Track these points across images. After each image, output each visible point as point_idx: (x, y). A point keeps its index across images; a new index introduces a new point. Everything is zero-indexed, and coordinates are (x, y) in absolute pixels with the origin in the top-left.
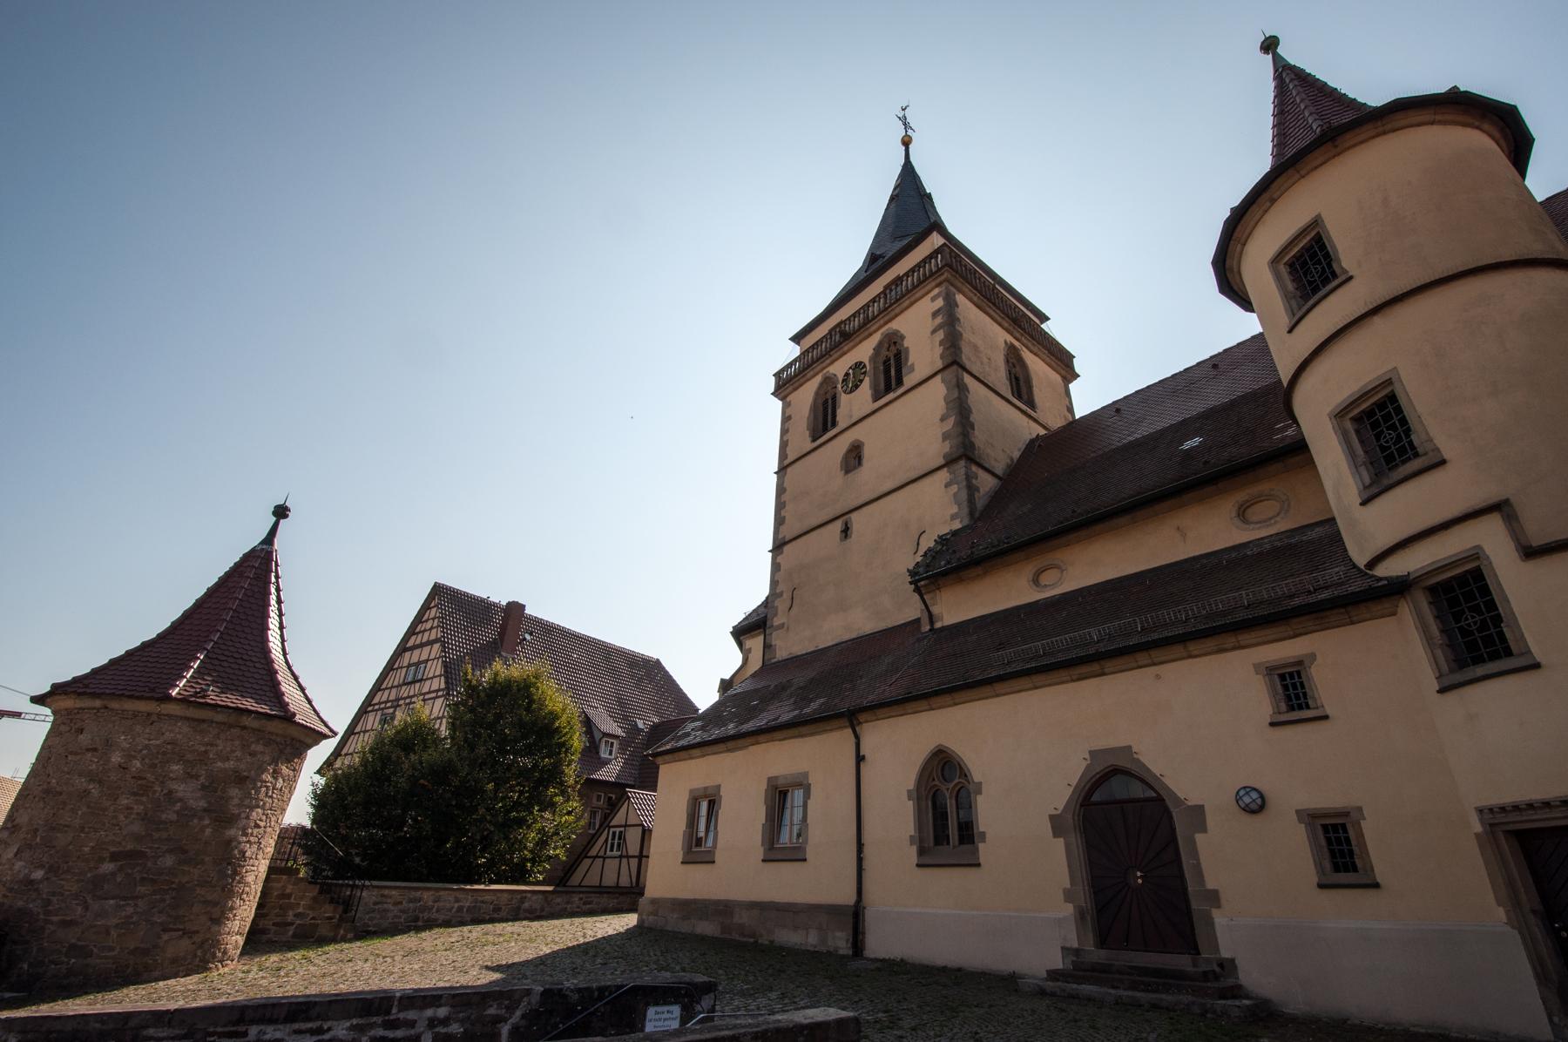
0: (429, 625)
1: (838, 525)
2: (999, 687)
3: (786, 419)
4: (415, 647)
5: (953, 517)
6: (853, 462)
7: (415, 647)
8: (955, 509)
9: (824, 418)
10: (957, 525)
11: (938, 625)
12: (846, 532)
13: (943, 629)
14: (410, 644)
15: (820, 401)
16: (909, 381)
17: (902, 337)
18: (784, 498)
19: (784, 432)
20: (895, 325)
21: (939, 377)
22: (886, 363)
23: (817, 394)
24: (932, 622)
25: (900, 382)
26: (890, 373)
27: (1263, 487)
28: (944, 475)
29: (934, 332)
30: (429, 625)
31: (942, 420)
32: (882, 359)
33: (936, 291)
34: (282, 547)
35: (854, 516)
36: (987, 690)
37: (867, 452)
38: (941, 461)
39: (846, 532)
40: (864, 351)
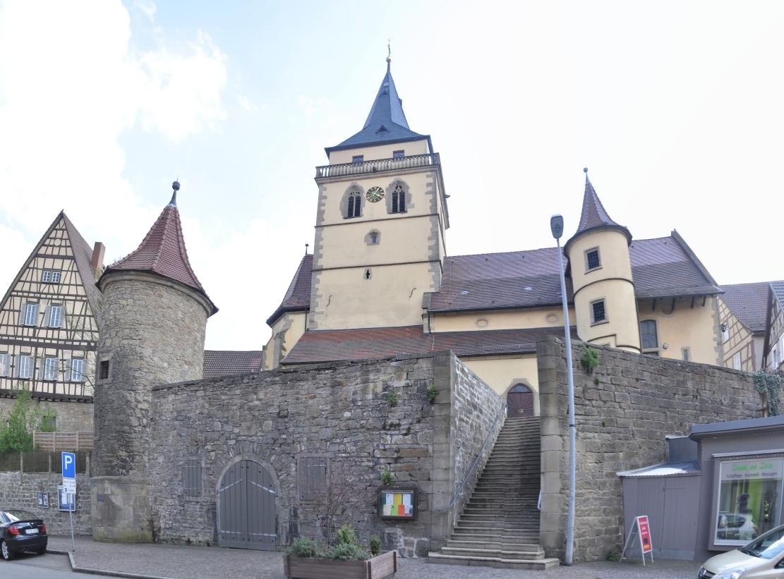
0: (57, 242)
1: (363, 271)
2: (487, 358)
3: (322, 198)
4: (45, 256)
5: (431, 286)
6: (371, 240)
7: (45, 256)
8: (433, 283)
9: (353, 208)
10: (433, 290)
11: (432, 331)
12: (368, 274)
13: (435, 333)
14: (42, 251)
15: (348, 197)
16: (410, 212)
17: (408, 187)
18: (321, 243)
19: (320, 205)
20: (404, 178)
21: (428, 218)
22: (395, 195)
23: (347, 192)
24: (430, 330)
25: (403, 210)
26: (399, 203)
27: (555, 312)
28: (428, 266)
29: (427, 193)
30: (57, 242)
31: (429, 239)
32: (392, 191)
33: (429, 173)
34: (180, 205)
35: (373, 270)
36: (483, 358)
37: (382, 238)
38: (427, 259)
39: (368, 274)
40: (385, 183)
